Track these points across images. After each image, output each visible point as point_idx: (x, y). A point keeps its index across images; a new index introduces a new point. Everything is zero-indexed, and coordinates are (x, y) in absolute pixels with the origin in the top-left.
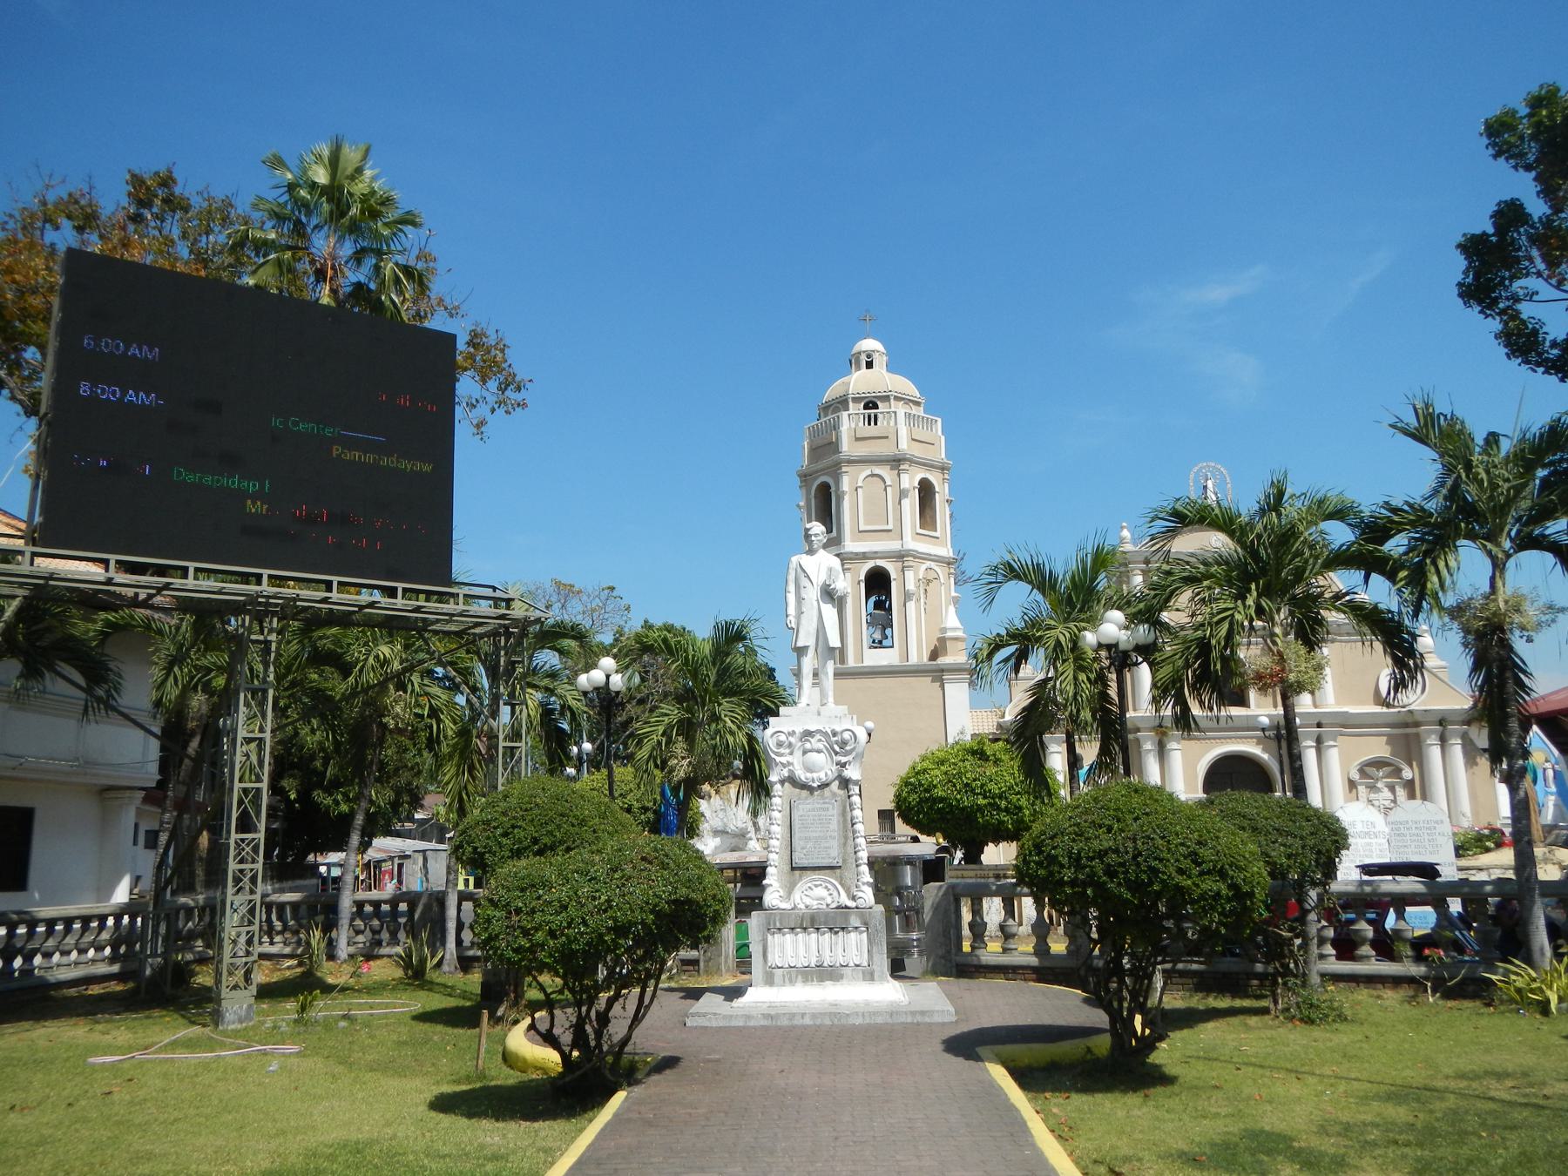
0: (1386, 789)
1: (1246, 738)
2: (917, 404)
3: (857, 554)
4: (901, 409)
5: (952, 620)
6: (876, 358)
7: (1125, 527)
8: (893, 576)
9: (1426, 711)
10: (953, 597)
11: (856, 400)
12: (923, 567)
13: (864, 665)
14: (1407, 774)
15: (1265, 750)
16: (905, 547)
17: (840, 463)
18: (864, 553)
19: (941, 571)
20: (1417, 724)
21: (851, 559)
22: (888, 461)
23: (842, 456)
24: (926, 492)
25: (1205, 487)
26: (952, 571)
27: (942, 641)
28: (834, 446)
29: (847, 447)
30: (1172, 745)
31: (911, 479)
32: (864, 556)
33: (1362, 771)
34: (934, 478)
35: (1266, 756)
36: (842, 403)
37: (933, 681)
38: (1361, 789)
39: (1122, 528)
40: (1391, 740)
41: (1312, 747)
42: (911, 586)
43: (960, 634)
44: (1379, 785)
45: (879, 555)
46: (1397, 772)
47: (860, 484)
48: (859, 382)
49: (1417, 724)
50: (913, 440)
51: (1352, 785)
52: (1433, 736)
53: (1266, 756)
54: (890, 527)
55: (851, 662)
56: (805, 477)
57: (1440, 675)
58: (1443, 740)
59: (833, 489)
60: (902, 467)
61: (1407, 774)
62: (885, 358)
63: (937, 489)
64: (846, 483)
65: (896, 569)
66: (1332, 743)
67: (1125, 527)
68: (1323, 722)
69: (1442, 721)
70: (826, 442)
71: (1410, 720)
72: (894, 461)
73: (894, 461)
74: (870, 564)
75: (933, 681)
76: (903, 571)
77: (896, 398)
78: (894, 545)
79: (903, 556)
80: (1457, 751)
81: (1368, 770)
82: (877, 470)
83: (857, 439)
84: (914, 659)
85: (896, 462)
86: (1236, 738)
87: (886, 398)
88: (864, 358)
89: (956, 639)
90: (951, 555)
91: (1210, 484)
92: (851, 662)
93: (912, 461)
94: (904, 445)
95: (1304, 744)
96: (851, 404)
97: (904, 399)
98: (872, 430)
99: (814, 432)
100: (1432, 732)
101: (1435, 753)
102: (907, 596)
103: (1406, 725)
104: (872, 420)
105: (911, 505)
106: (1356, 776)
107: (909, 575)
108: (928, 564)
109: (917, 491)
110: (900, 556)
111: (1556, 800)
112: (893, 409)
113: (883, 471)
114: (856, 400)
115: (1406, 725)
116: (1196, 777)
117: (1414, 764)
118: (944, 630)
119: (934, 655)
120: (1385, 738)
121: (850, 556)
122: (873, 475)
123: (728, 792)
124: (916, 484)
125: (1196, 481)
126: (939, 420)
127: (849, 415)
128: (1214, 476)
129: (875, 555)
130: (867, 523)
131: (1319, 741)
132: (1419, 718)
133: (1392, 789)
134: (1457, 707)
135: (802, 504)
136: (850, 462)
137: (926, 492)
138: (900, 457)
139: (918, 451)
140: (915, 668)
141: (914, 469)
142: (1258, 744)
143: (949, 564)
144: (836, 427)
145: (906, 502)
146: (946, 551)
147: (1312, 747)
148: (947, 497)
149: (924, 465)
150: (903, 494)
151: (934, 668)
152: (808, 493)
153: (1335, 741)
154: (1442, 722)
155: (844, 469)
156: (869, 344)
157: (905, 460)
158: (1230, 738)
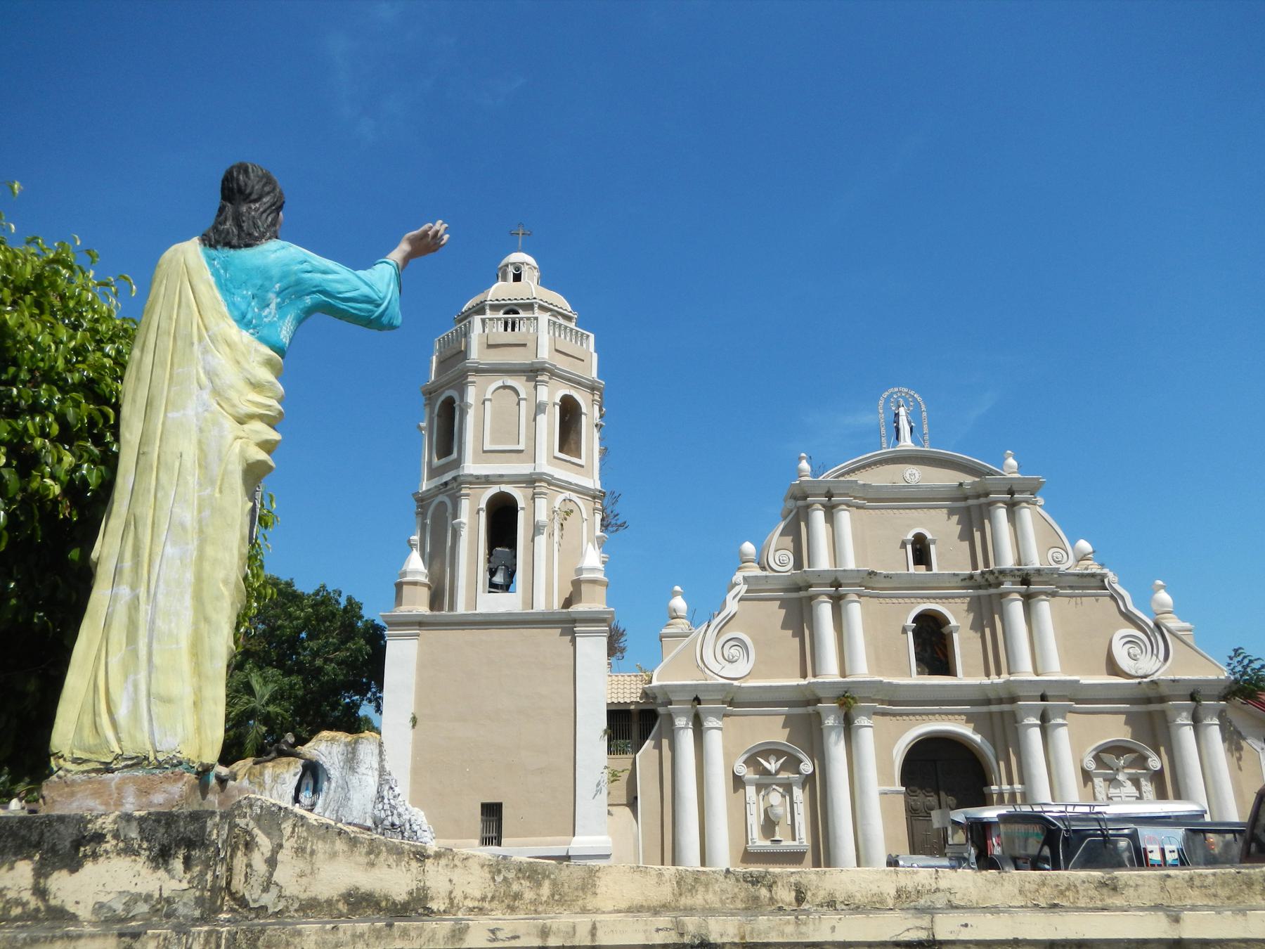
0: (1129, 783)
1: (953, 714)
2: (569, 318)
3: (478, 477)
4: (544, 318)
5: (593, 559)
6: (525, 269)
7: (803, 458)
8: (521, 504)
9: (1174, 681)
10: (598, 538)
11: (495, 308)
12: (561, 497)
13: (477, 612)
14: (1154, 763)
15: (976, 730)
16: (537, 471)
17: (468, 371)
18: (488, 476)
19: (584, 505)
20: (1162, 699)
21: (471, 483)
22: (524, 371)
23: (468, 363)
24: (570, 412)
25: (897, 415)
26: (598, 506)
27: (577, 584)
28: (463, 354)
29: (476, 354)
30: (862, 721)
31: (551, 394)
32: (487, 480)
33: (1097, 758)
34: (582, 397)
35: (978, 738)
36: (480, 309)
37: (562, 634)
38: (1098, 781)
39: (800, 459)
40: (1131, 719)
41: (1035, 725)
42: (542, 516)
43: (600, 576)
45: (505, 479)
46: (1141, 761)
47: (488, 396)
48: (501, 290)
49: (1162, 699)
50: (557, 351)
51: (1087, 776)
52: (1184, 714)
53: (978, 738)
54: (521, 447)
55: (461, 608)
56: (430, 393)
57: (1183, 637)
58: (1196, 721)
59: (457, 403)
60: (539, 378)
61: (1154, 763)
62: (536, 274)
63: (584, 410)
64: (472, 395)
65: (525, 497)
66: (1060, 721)
67: (803, 458)
68: (1048, 693)
69: (1194, 694)
70: (454, 351)
71: (1152, 694)
72: (531, 371)
73: (531, 371)
74: (494, 490)
75: (562, 634)
76: (533, 499)
77: (542, 308)
78: (524, 469)
79: (535, 482)
80: (1214, 733)
81: (1106, 757)
82: (510, 381)
83: (490, 346)
84: (540, 606)
85: (533, 372)
86: (940, 714)
87: (529, 307)
88: (511, 271)
89: (594, 582)
90: (598, 487)
91: (902, 411)
92: (461, 608)
93: (553, 373)
94: (545, 354)
95: (1026, 722)
96: (488, 311)
97: (550, 310)
98: (509, 337)
99: (446, 343)
100: (1182, 708)
101: (1187, 735)
102: (537, 529)
103: (1149, 701)
104: (511, 326)
105: (549, 424)
106: (1091, 765)
107: (541, 504)
108: (567, 494)
109: (557, 408)
110: (531, 481)
112: (536, 315)
113: (519, 383)
114: (495, 308)
115: (1149, 701)
116: (892, 763)
117: (1162, 749)
118: (580, 571)
119: (568, 603)
121: (470, 479)
122: (505, 387)
123: (261, 774)
124: (558, 400)
125: (886, 408)
126: (592, 336)
127: (483, 321)
128: (907, 403)
129: (500, 479)
130: (493, 441)
131: (1044, 718)
132: (1165, 691)
133: (1136, 782)
134: (1211, 677)
135: (423, 424)
136: (478, 371)
137: (570, 412)
138: (538, 366)
139: (562, 363)
140: (541, 617)
141: (554, 382)
142: (968, 721)
143: (594, 497)
144: (466, 334)
145: (542, 419)
146: (594, 483)
147: (1035, 725)
148: (598, 421)
149: (569, 380)
150: (540, 408)
151: (563, 617)
152: (432, 412)
153: (1064, 718)
154: (1193, 697)
155: (470, 379)
156: (517, 257)
158: (933, 714)
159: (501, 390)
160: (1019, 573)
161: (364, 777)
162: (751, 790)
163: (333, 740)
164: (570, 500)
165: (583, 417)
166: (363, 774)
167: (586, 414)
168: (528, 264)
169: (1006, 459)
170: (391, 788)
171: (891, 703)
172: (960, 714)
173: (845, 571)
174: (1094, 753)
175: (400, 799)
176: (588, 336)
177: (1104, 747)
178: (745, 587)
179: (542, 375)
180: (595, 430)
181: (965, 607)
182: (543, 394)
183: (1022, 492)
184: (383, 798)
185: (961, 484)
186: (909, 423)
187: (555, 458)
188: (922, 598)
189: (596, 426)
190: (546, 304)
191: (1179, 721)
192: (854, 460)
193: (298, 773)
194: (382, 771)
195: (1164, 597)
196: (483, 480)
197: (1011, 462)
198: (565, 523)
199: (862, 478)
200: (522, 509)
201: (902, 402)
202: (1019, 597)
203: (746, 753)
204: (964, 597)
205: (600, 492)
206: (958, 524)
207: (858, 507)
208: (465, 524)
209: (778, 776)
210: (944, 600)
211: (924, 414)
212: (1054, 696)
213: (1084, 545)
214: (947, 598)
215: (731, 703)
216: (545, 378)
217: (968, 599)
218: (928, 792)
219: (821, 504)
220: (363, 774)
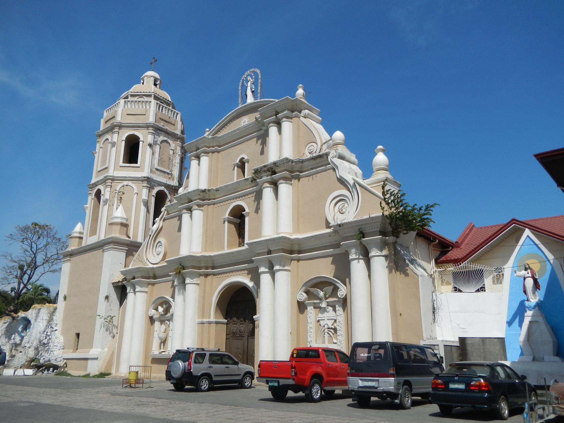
0: (330, 309)
6: (145, 78)
8: (102, 193)
12: (122, 185)
18: (95, 183)
38: (310, 309)
44: (324, 305)
47: (102, 146)
63: (141, 139)
82: (108, 136)
93: (120, 126)
94: (119, 119)
106: (303, 296)
108: (126, 183)
109: (124, 142)
111: (533, 316)
120: (331, 258)
124: (124, 138)
142: (248, 274)
143: (143, 181)
146: (145, 173)
149: (133, 127)
150: (113, 144)
157: (116, 126)
158: (232, 272)
159: (106, 141)
160: (266, 169)
161: (38, 323)
162: (157, 324)
163: (34, 308)
164: (127, 185)
165: (141, 143)
166: (38, 322)
167: (141, 141)
168: (146, 76)
169: (298, 90)
170: (51, 327)
171: (213, 268)
172: (244, 270)
173: (189, 193)
174: (304, 288)
175: (56, 332)
176: (150, 102)
177: (315, 281)
178: (166, 212)
179: (115, 129)
180: (148, 147)
181: (253, 199)
182: (115, 137)
183: (283, 111)
184: (45, 331)
185: (256, 118)
186: (251, 89)
187: (121, 167)
188: (233, 199)
189: (148, 145)
190: (134, 93)
191: (351, 257)
192: (217, 124)
193: (7, 322)
194: (50, 320)
195: (381, 158)
196: (94, 186)
197: (300, 92)
198: (123, 196)
199: (220, 134)
200: (102, 195)
201: (249, 78)
202: (269, 185)
203: (153, 303)
204: (253, 193)
205: (144, 177)
206: (261, 145)
207: (213, 152)
208: (88, 207)
209: (166, 316)
210: (244, 198)
211: (260, 80)
212: (274, 250)
213: (339, 135)
214: (245, 196)
215: (155, 277)
216: (116, 130)
217: (255, 193)
218: (242, 321)
219: (194, 156)
220: (38, 322)
